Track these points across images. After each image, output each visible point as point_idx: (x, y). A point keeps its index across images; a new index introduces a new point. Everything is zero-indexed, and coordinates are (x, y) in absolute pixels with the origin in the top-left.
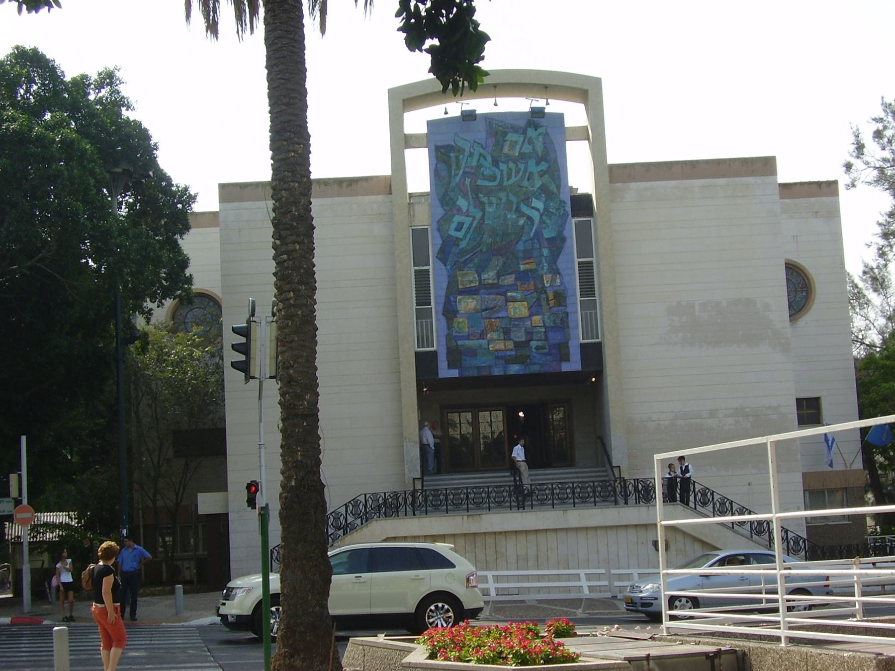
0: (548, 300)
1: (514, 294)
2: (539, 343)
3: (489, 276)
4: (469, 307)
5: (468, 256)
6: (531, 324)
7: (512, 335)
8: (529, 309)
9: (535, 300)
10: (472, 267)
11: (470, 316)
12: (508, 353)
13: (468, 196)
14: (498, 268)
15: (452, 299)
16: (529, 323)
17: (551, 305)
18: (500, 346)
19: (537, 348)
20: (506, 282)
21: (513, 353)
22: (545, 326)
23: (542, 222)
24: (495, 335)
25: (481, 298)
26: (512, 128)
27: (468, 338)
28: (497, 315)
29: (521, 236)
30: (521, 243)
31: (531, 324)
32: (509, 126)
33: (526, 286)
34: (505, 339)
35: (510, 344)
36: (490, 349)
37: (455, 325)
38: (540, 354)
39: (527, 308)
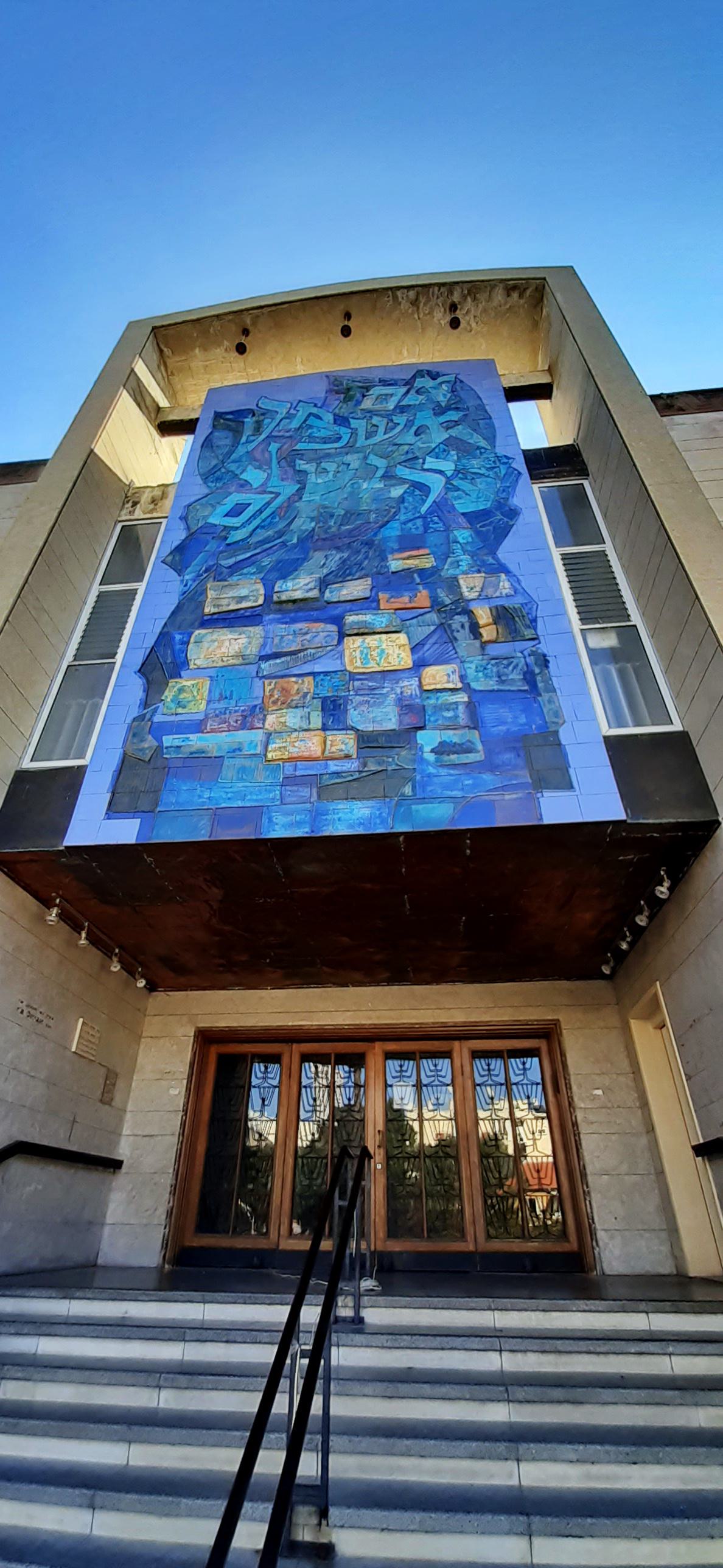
0: (475, 629)
1: (368, 618)
2: (452, 737)
3: (298, 586)
4: (223, 650)
5: (248, 555)
6: (420, 685)
7: (354, 717)
8: (413, 650)
9: (432, 628)
10: (254, 573)
11: (220, 675)
12: (333, 767)
13: (269, 463)
14: (325, 571)
15: (178, 637)
16: (415, 682)
17: (485, 638)
18: (312, 745)
19: (442, 749)
20: (344, 592)
21: (353, 765)
22: (467, 688)
23: (449, 486)
24: (292, 718)
25: (267, 632)
26: (380, 381)
27: (198, 727)
28: (307, 668)
29: (395, 514)
30: (395, 524)
31: (420, 685)
32: (377, 380)
33: (406, 599)
34: (324, 728)
35: (343, 742)
36: (269, 756)
37: (169, 695)
38: (455, 766)
39: (408, 648)
